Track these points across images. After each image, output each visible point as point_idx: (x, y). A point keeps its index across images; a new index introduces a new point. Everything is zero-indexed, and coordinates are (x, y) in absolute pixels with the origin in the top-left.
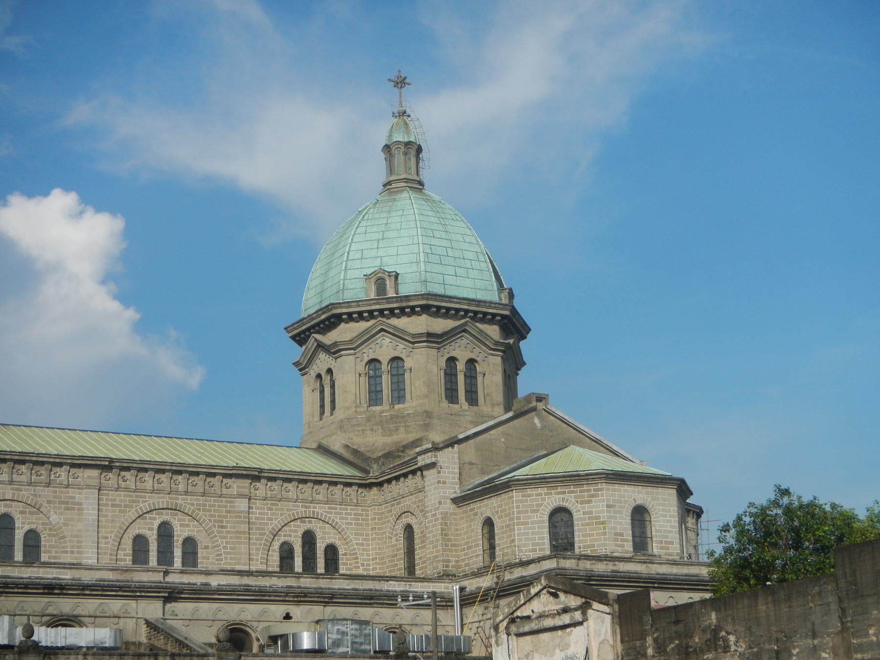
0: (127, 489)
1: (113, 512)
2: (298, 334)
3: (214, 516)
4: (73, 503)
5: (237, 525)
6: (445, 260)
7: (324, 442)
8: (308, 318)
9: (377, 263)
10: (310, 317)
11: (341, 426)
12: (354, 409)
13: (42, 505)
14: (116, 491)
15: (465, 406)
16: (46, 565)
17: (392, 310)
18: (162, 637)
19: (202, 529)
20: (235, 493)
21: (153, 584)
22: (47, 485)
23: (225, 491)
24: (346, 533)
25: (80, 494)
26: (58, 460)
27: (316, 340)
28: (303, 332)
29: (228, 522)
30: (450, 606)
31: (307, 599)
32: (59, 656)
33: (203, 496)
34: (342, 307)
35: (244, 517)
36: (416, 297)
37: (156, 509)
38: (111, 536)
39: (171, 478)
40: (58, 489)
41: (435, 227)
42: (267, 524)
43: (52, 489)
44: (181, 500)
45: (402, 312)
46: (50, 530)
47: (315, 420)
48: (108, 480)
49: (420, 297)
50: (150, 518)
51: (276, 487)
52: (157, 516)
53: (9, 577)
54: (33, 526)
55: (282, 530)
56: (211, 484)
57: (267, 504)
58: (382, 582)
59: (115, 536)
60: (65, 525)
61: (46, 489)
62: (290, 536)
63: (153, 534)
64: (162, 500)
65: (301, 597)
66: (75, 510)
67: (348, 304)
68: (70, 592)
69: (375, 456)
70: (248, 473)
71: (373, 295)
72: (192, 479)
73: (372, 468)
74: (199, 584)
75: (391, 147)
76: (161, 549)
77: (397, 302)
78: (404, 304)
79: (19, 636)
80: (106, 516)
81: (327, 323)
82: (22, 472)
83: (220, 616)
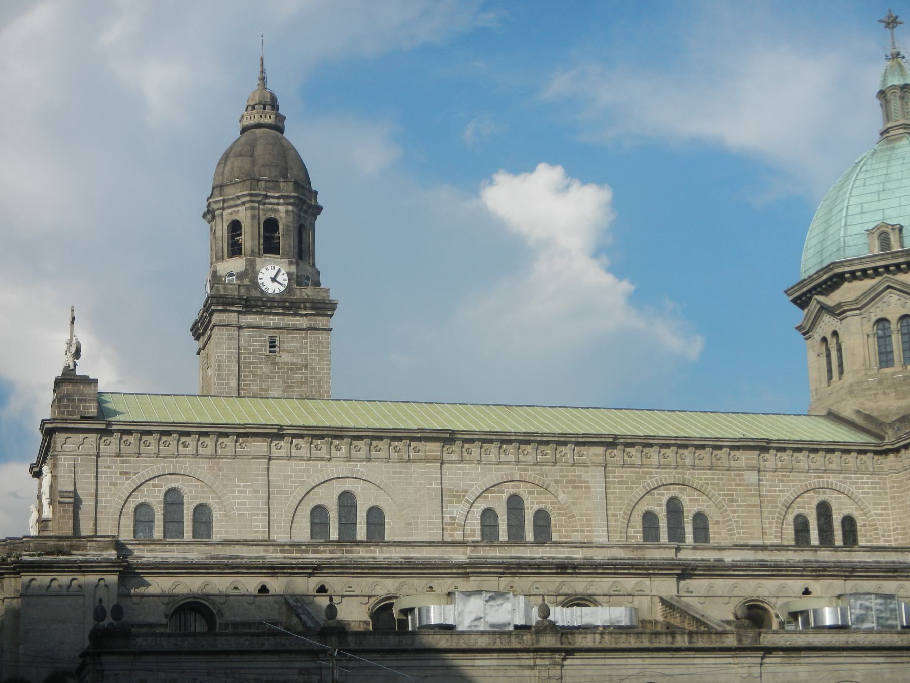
0: (633, 465)
1: (621, 488)
2: (799, 297)
3: (723, 490)
4: (580, 482)
5: (748, 498)
7: (834, 409)
8: (809, 280)
10: (811, 278)
11: (851, 392)
12: (864, 372)
13: (549, 484)
14: (622, 468)
16: (557, 544)
17: (898, 266)
18: (678, 615)
20: (744, 465)
21: (665, 561)
22: (553, 464)
23: (732, 464)
25: (586, 472)
26: (562, 439)
27: (818, 302)
28: (805, 294)
31: (826, 573)
32: (576, 635)
33: (710, 470)
35: (755, 490)
37: (664, 485)
38: (620, 514)
39: (677, 453)
40: (564, 468)
42: (779, 496)
43: (558, 468)
44: (688, 475)
47: (823, 386)
48: (614, 457)
53: (522, 558)
54: (542, 506)
55: (795, 502)
56: (718, 457)
57: (777, 476)
58: (906, 553)
60: (574, 503)
62: (804, 508)
63: (662, 510)
64: (670, 476)
65: (819, 571)
66: (582, 488)
67: (851, 262)
68: (582, 571)
69: (889, 421)
70: (756, 444)
71: (876, 251)
72: (698, 452)
73: (887, 433)
74: (712, 560)
75: (886, 92)
76: (670, 525)
77: (903, 256)
80: (614, 493)
83: (736, 592)
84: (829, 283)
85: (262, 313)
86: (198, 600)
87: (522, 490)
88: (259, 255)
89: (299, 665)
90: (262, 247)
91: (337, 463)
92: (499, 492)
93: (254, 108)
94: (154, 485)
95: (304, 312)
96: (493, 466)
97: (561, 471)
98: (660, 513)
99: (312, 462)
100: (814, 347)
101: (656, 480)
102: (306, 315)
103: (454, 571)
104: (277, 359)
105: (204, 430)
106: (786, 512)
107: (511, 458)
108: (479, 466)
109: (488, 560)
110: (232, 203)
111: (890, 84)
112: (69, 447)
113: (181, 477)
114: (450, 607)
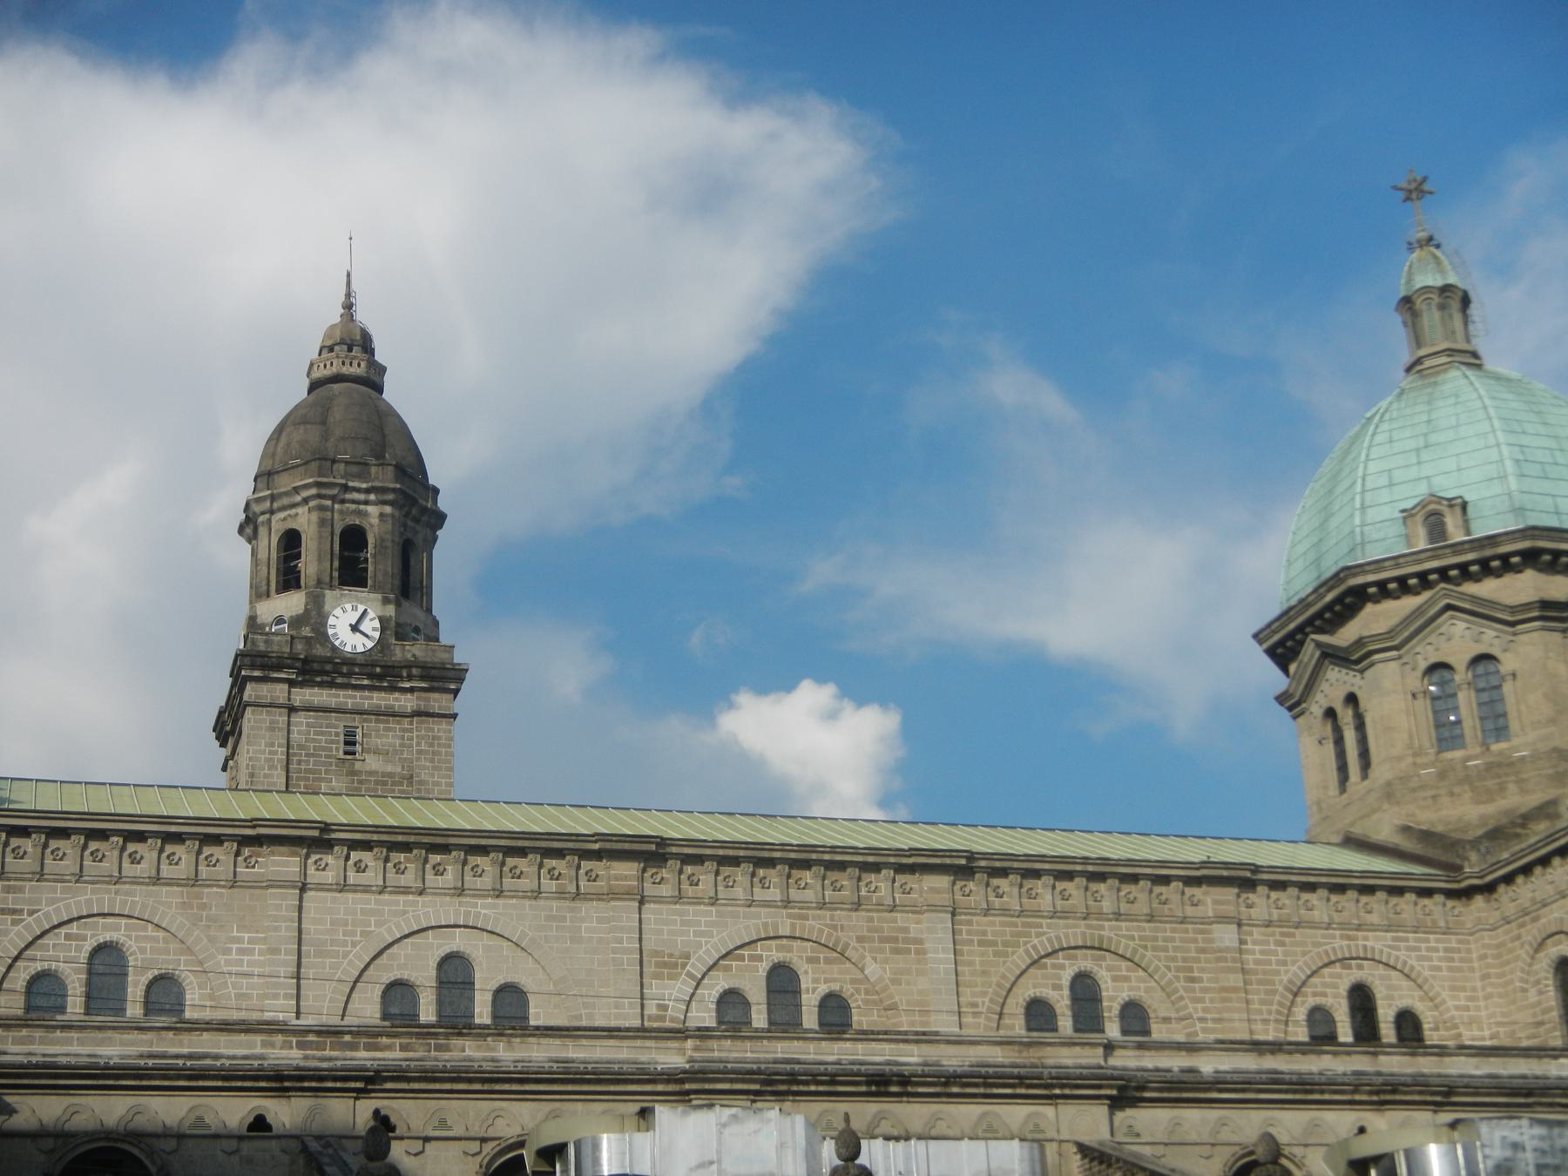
0: (1005, 911)
1: (983, 955)
2: (1281, 643)
3: (1174, 959)
4: (906, 941)
7: (1357, 830)
8: (1300, 607)
9: (1422, 490)
10: (1304, 603)
11: (1389, 793)
12: (1410, 760)
13: (848, 944)
14: (985, 915)
16: (867, 1035)
17: (1463, 568)
19: (1153, 984)
20: (1210, 914)
22: (855, 906)
23: (1190, 911)
24: (1432, 987)
25: (917, 923)
26: (871, 859)
27: (1318, 645)
28: (1291, 636)
29: (1202, 970)
31: (1398, 1097)
33: (1149, 921)
34: (1366, 572)
35: (1234, 960)
36: (1510, 537)
37: (1063, 949)
38: (983, 1003)
40: (875, 915)
42: (1278, 973)
43: (864, 913)
44: (1108, 931)
45: (1486, 569)
46: (867, 992)
48: (968, 895)
49: (1517, 535)
50: (1054, 966)
51: (1287, 902)
52: (1067, 962)
53: (798, 1062)
54: (835, 987)
55: (1308, 984)
56: (1163, 898)
57: (1273, 934)
58: (1546, 1060)
59: (991, 1001)
60: (895, 982)
61: (854, 914)
62: (1324, 995)
63: (1062, 996)
64: (1075, 932)
65: (1384, 1092)
66: (910, 953)
67: (1378, 564)
68: (921, 1090)
69: (1470, 835)
71: (1422, 544)
72: (1126, 888)
73: (1467, 859)
74: (1176, 1069)
75: (1414, 297)
76: (1079, 1026)
77: (1471, 550)
78: (1488, 553)
80: (971, 963)
81: (1338, 608)
82: (806, 884)
83: (1226, 1135)
84: (1338, 608)
85: (332, 685)
86: (119, 1145)
87: (797, 956)
88: (331, 587)
90: (336, 574)
91: (438, 899)
92: (753, 958)
93: (331, 349)
94: (68, 937)
95: (407, 685)
96: (738, 909)
97: (871, 920)
98: (1058, 1001)
99: (386, 897)
100: (1311, 728)
101: (1050, 940)
102: (411, 690)
103: (660, 1088)
104: (358, 765)
105: (173, 829)
106: (1293, 1002)
107: (775, 894)
108: (713, 909)
109: (729, 1066)
110: (286, 501)
111: (1418, 286)
113: (124, 921)
114: (643, 1140)
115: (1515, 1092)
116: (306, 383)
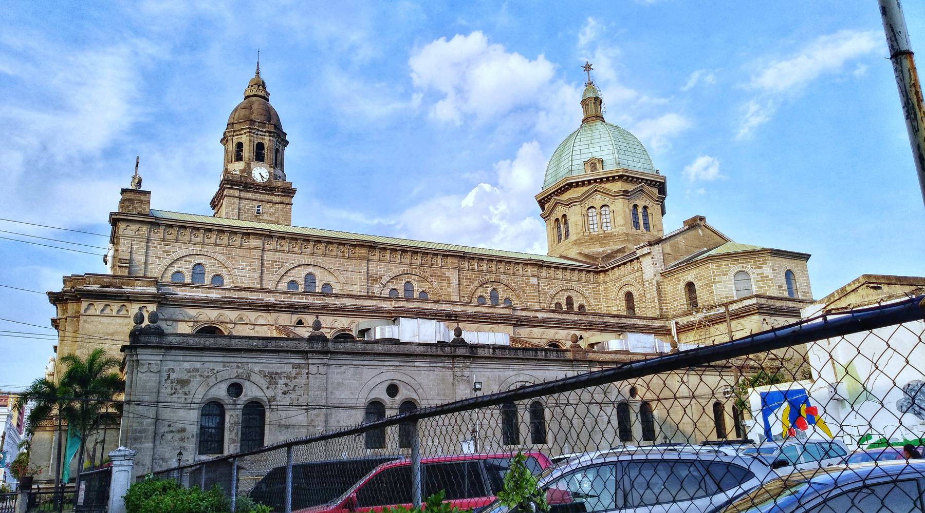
4: (445, 277)
6: (627, 153)
7: (564, 254)
9: (590, 156)
12: (582, 234)
15: (645, 231)
26: (436, 252)
27: (555, 199)
28: (547, 197)
30: (668, 334)
41: (619, 136)
57: (547, 281)
62: (560, 299)
70: (537, 263)
79: (452, 336)
83: (544, 336)
85: (253, 192)
86: (215, 325)
89: (293, 361)
90: (255, 157)
91: (305, 256)
93: (252, 86)
95: (277, 194)
99: (289, 254)
102: (278, 195)
104: (261, 217)
105: (221, 229)
106: (551, 301)
110: (238, 133)
112: (129, 232)
114: (395, 328)
115: (622, 327)
116: (244, 97)
